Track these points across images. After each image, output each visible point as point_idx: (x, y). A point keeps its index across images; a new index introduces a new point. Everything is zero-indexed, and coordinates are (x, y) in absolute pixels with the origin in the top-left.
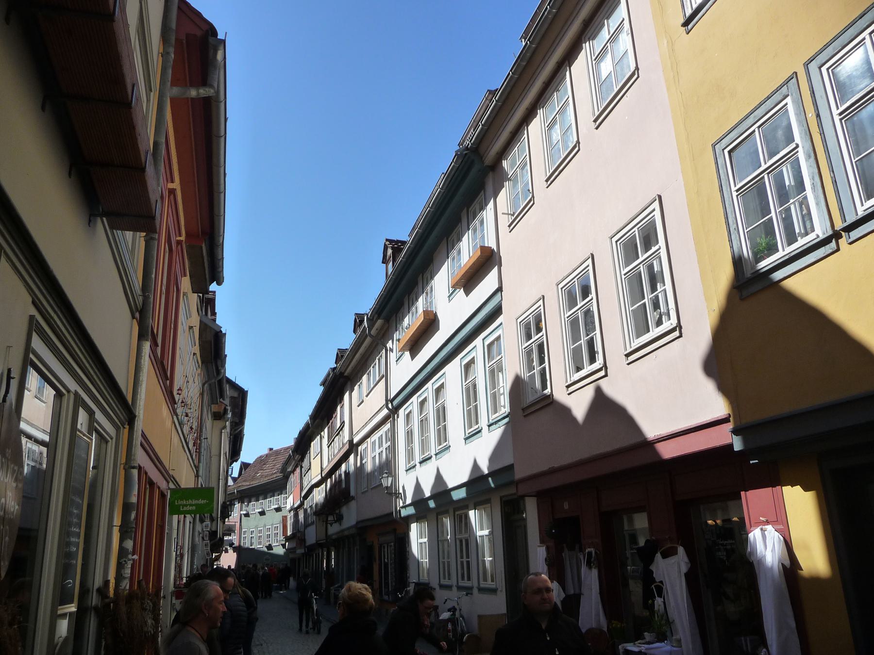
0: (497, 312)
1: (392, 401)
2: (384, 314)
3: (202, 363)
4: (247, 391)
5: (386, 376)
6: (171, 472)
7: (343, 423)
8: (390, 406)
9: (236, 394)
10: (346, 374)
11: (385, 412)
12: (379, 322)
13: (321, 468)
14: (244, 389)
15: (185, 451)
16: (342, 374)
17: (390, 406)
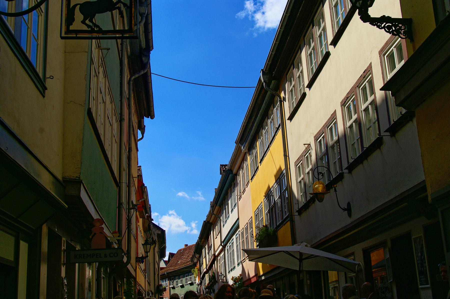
0: (238, 227)
1: (223, 242)
2: (218, 204)
3: (144, 232)
4: (165, 230)
5: (220, 232)
6: (139, 283)
7: (211, 245)
8: (223, 244)
9: (160, 232)
10: (211, 221)
11: (221, 247)
12: (217, 208)
13: (206, 264)
14: (163, 230)
15: (141, 272)
16: (208, 222)
17: (223, 244)
